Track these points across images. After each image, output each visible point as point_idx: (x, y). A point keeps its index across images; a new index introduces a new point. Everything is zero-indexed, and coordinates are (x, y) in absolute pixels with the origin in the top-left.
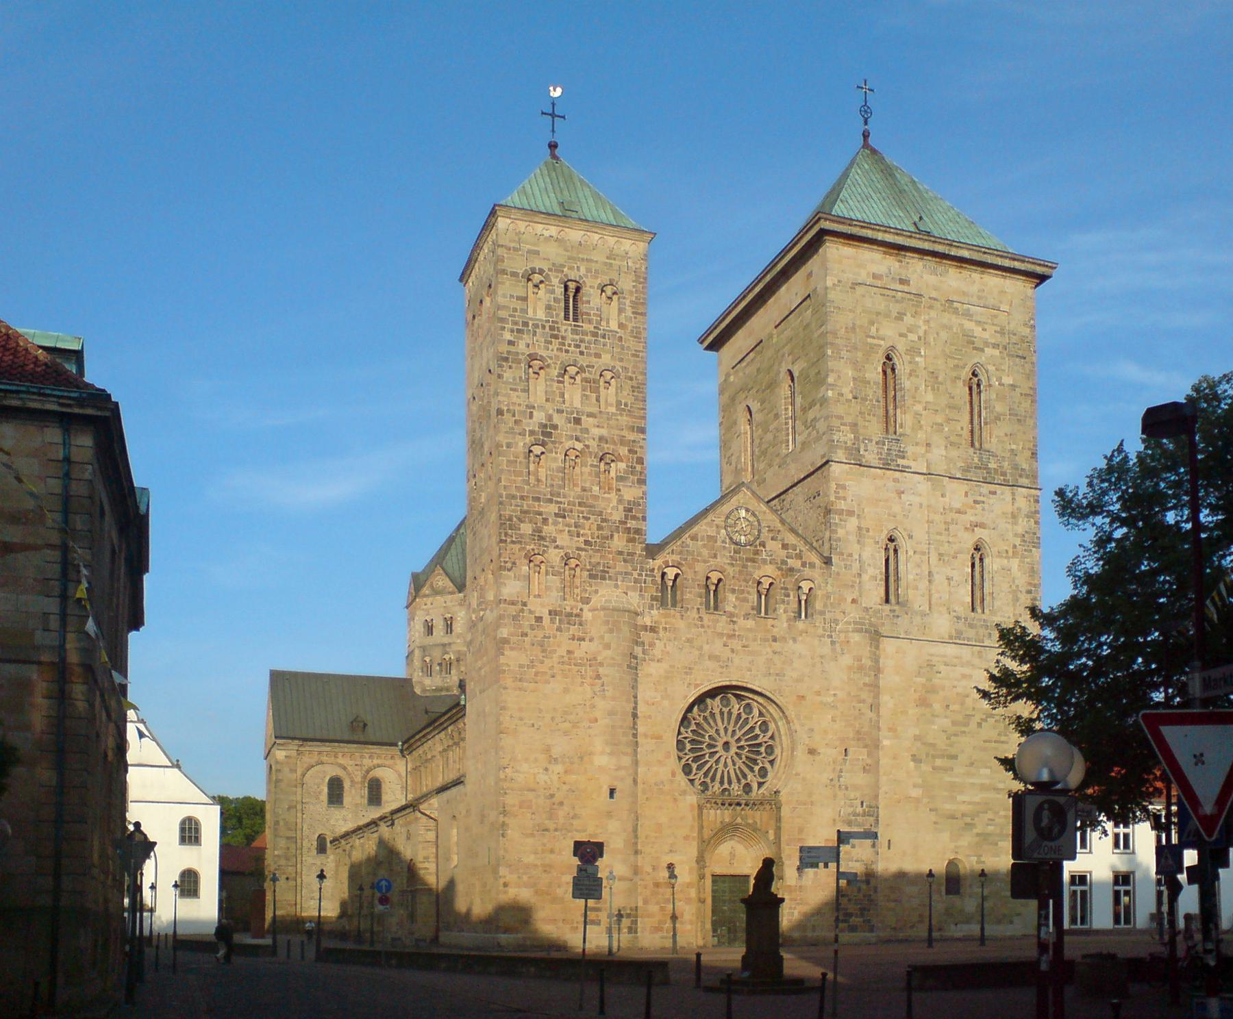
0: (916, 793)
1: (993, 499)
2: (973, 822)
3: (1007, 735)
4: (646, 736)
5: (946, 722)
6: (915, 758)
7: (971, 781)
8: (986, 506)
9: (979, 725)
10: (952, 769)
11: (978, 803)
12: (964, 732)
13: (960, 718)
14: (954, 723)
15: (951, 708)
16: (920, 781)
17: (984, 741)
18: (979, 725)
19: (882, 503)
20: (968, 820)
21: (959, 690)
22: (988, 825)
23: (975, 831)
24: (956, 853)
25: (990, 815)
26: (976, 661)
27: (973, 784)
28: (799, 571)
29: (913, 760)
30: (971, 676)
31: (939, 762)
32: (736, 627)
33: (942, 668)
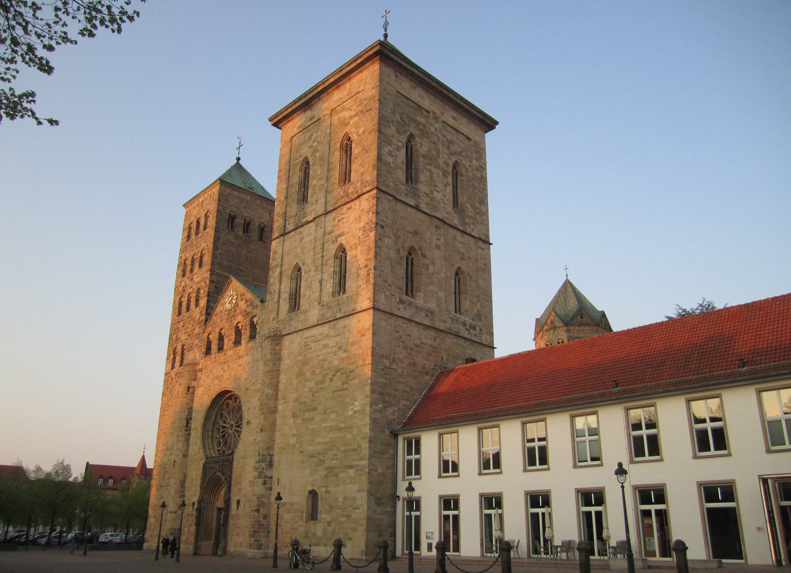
0: (293, 441)
1: (350, 212)
2: (324, 458)
3: (348, 383)
4: (193, 429)
5: (311, 384)
6: (294, 416)
7: (324, 425)
8: (345, 220)
9: (331, 380)
10: (313, 418)
11: (326, 443)
12: (322, 388)
13: (320, 378)
14: (317, 383)
15: (316, 372)
16: (295, 431)
17: (334, 392)
18: (331, 380)
19: (292, 252)
20: (321, 457)
21: (321, 357)
22: (333, 459)
23: (325, 465)
24: (314, 485)
25: (334, 452)
26: (332, 333)
27: (325, 428)
28: (251, 312)
29: (292, 417)
30: (328, 345)
31: (307, 415)
32: (226, 357)
33: (312, 345)
